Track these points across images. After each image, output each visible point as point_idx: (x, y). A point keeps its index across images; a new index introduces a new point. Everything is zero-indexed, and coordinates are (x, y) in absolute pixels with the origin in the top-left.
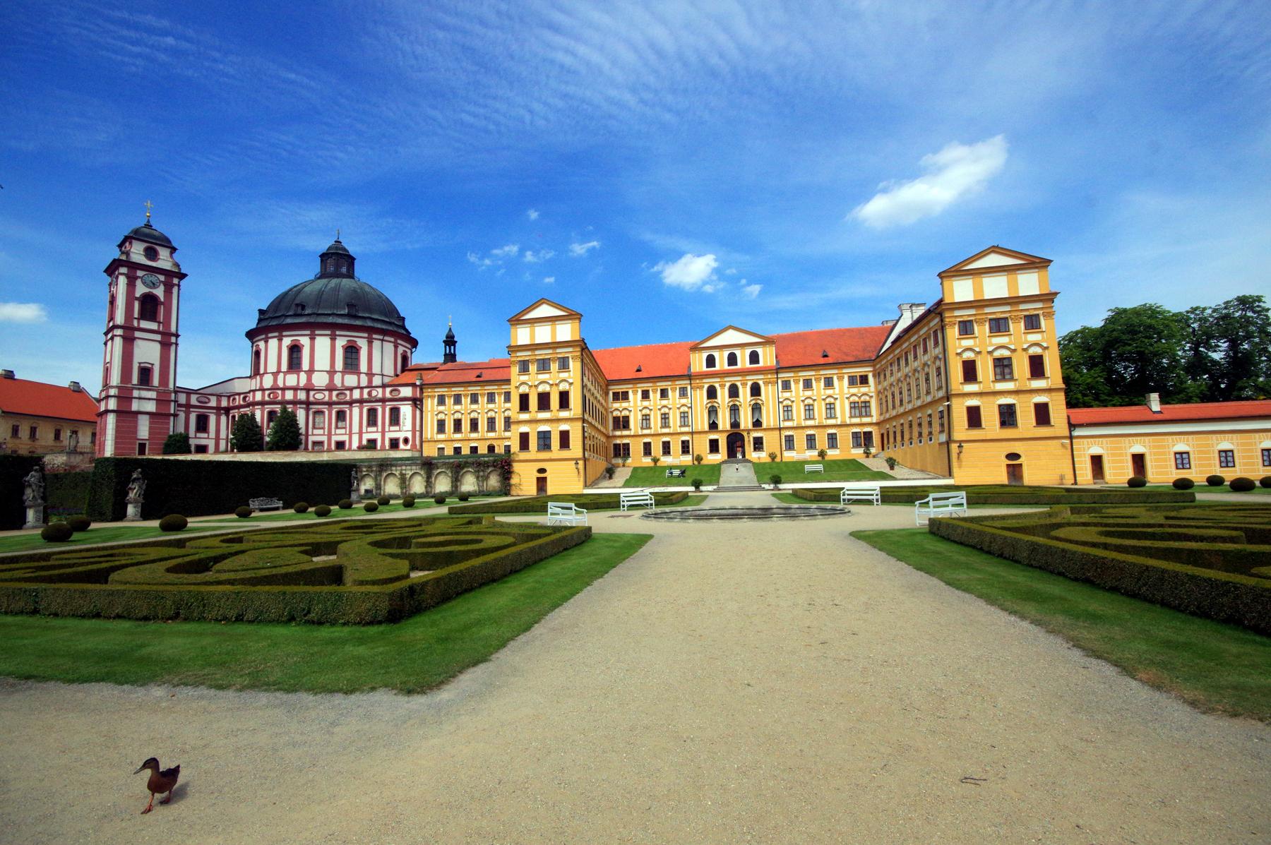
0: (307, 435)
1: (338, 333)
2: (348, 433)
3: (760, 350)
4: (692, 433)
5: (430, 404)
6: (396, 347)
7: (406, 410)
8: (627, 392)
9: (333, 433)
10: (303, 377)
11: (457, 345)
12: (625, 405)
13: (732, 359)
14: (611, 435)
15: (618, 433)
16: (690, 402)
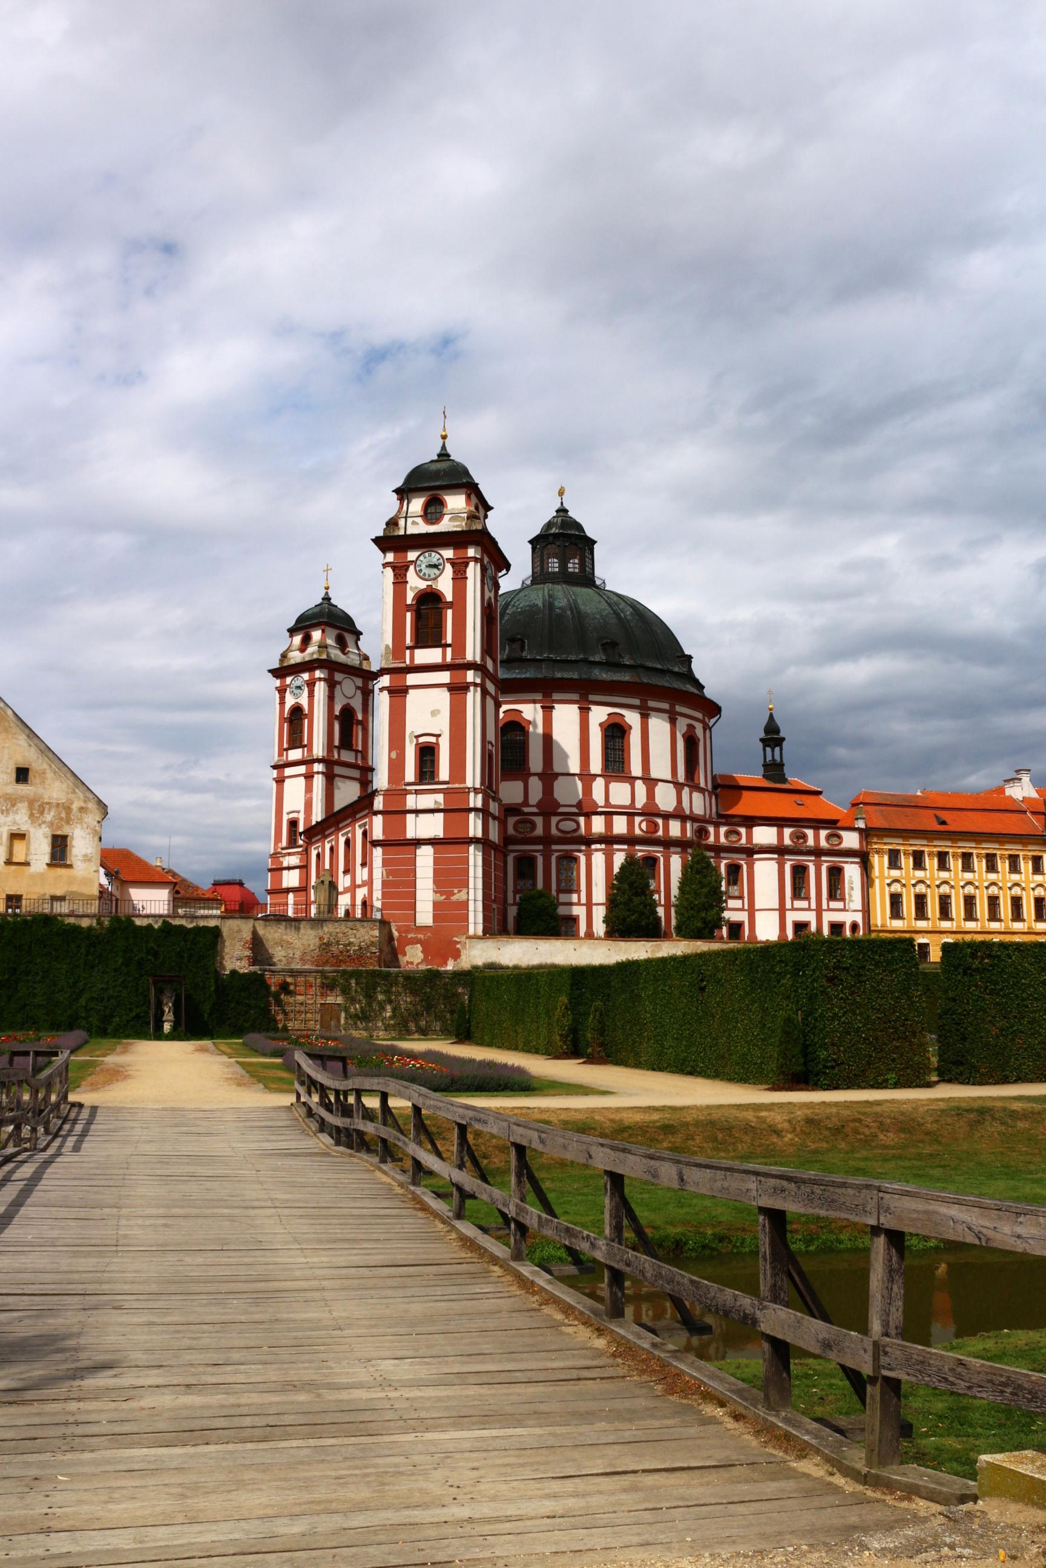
2: (746, 907)
5: (879, 863)
7: (852, 872)
11: (785, 744)
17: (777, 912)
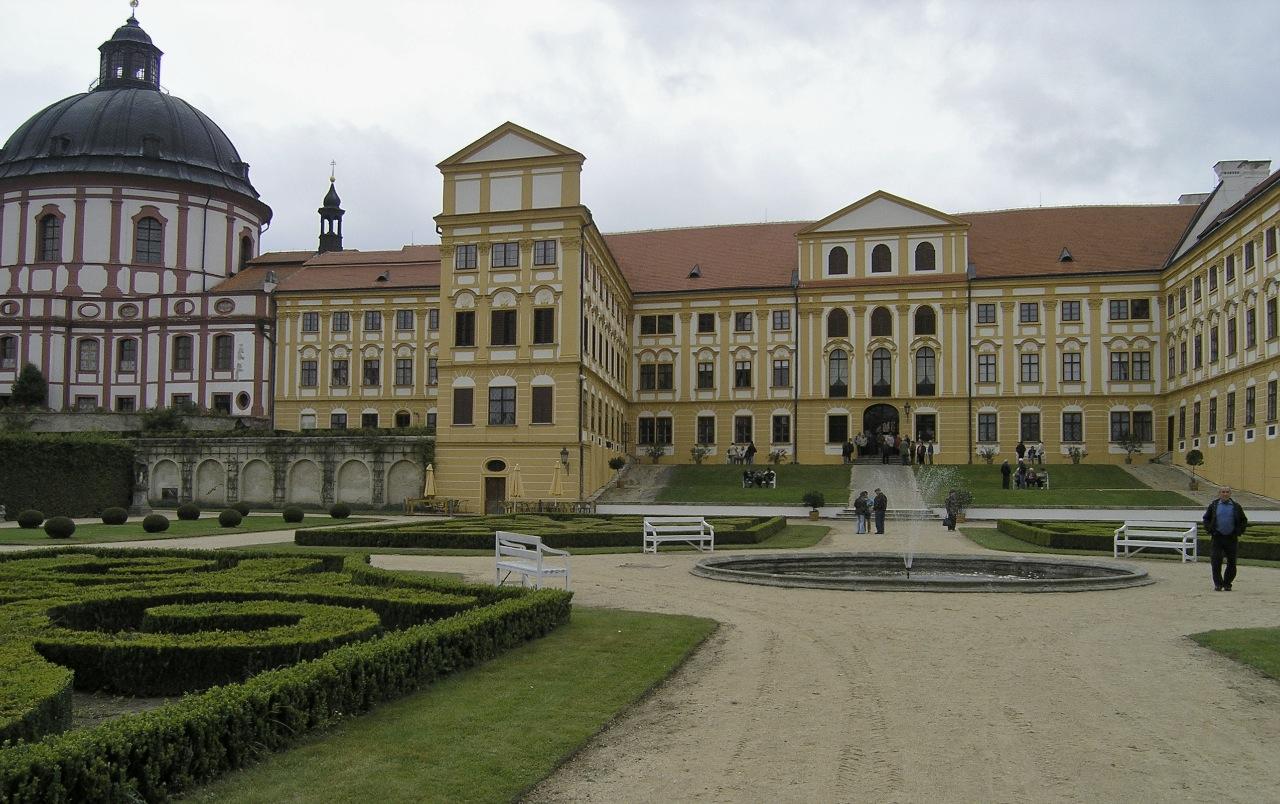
0: (67, 384)
1: (125, 192)
2: (139, 382)
3: (937, 243)
4: (796, 402)
5: (289, 330)
6: (230, 221)
7: (244, 341)
8: (670, 318)
9: (113, 381)
10: (62, 273)
12: (665, 341)
13: (881, 258)
14: (635, 400)
15: (649, 397)
16: (794, 340)
17: (157, 385)
